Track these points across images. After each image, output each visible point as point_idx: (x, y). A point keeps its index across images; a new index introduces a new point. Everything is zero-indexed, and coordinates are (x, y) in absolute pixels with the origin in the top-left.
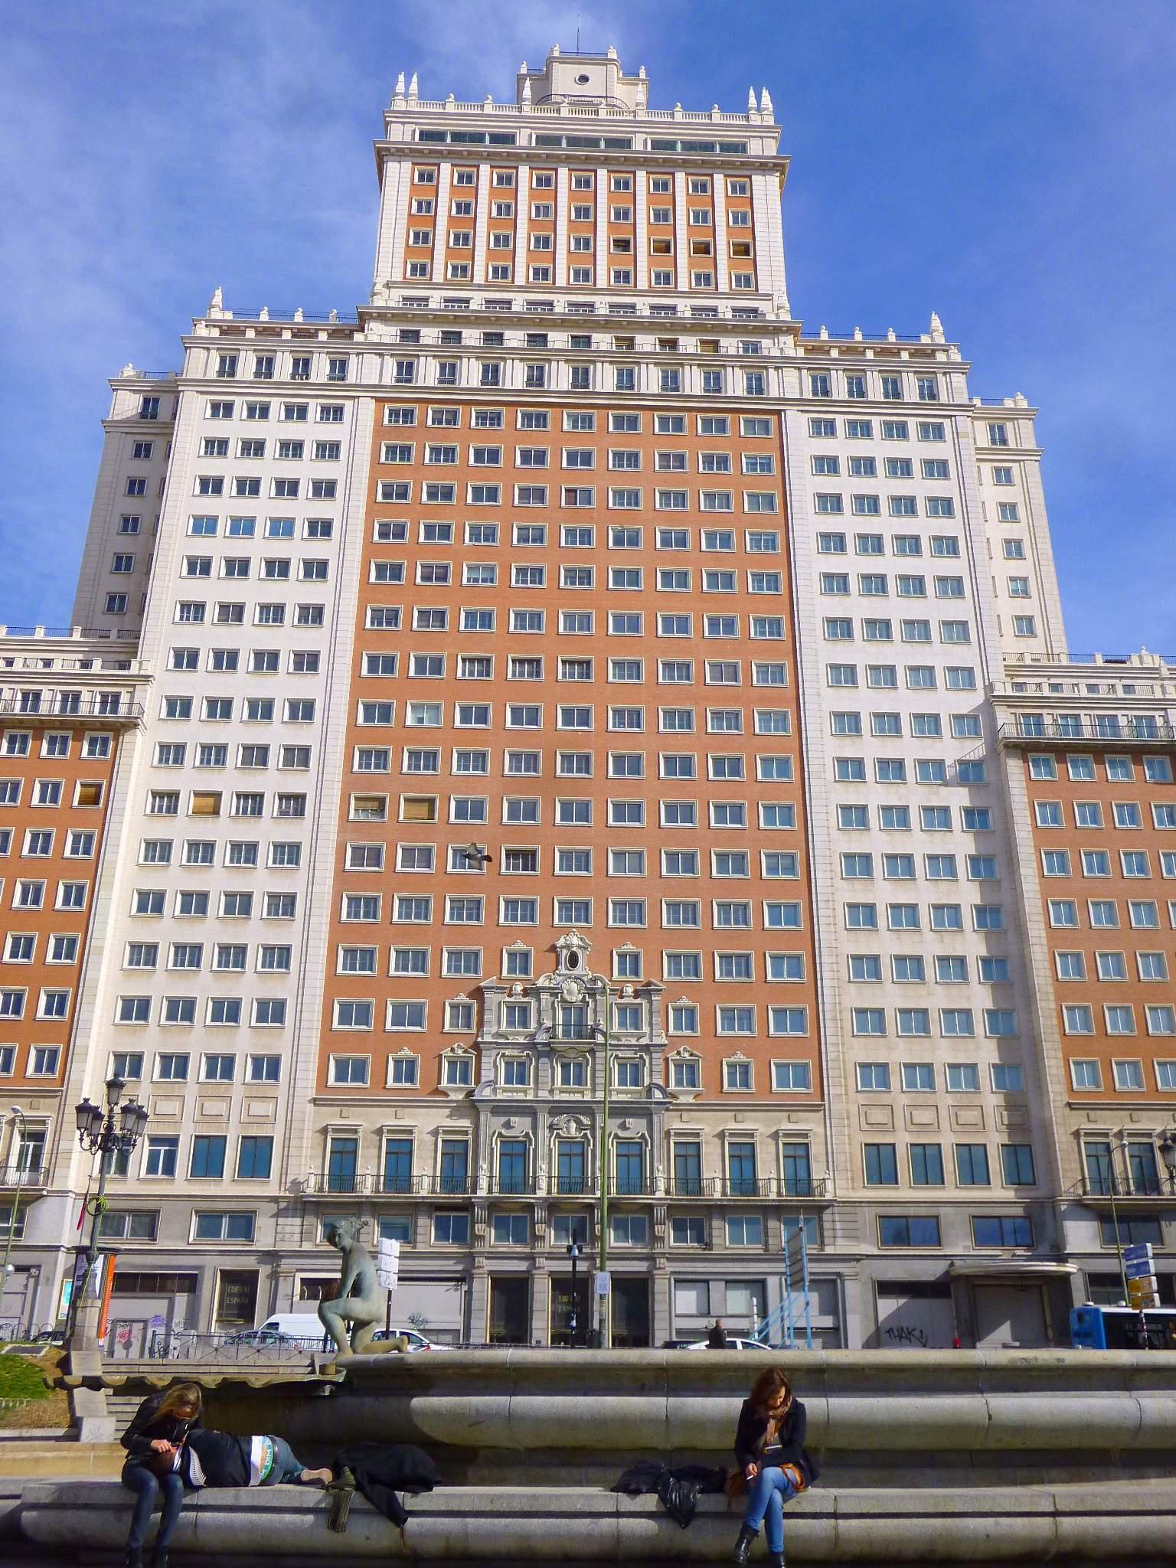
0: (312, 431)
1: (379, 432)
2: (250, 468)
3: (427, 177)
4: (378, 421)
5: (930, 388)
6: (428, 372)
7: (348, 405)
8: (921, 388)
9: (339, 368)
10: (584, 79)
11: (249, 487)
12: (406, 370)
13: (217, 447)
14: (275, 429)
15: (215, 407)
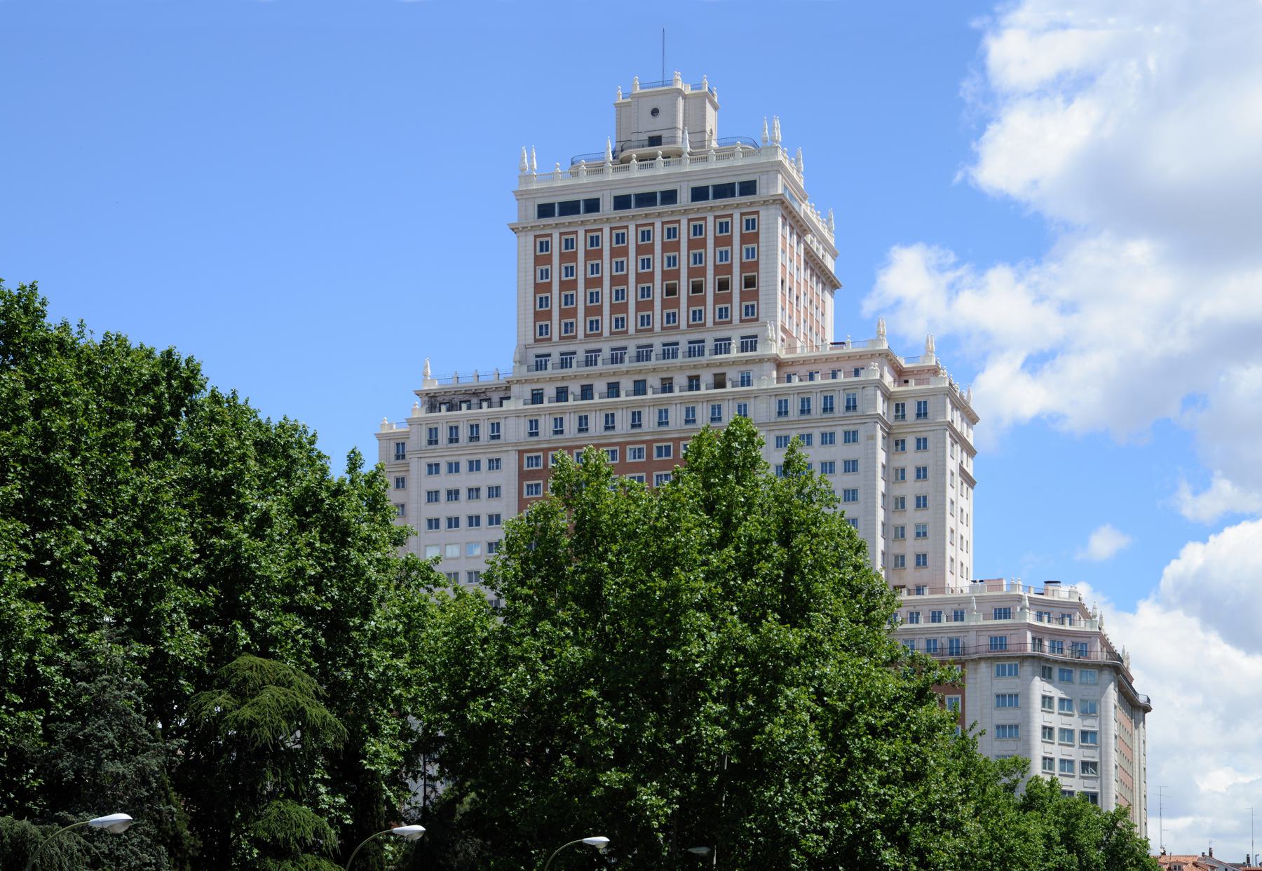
0: (484, 479)
1: (523, 475)
2: (454, 509)
3: (545, 246)
4: (521, 467)
5: (854, 400)
6: (546, 426)
7: (504, 458)
8: (848, 401)
9: (496, 427)
10: (655, 112)
11: (453, 522)
12: (534, 424)
13: (433, 496)
14: (463, 481)
15: (430, 466)
